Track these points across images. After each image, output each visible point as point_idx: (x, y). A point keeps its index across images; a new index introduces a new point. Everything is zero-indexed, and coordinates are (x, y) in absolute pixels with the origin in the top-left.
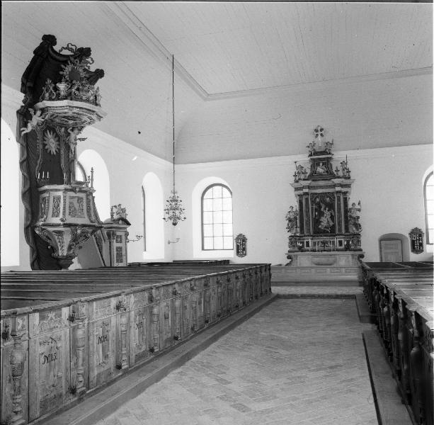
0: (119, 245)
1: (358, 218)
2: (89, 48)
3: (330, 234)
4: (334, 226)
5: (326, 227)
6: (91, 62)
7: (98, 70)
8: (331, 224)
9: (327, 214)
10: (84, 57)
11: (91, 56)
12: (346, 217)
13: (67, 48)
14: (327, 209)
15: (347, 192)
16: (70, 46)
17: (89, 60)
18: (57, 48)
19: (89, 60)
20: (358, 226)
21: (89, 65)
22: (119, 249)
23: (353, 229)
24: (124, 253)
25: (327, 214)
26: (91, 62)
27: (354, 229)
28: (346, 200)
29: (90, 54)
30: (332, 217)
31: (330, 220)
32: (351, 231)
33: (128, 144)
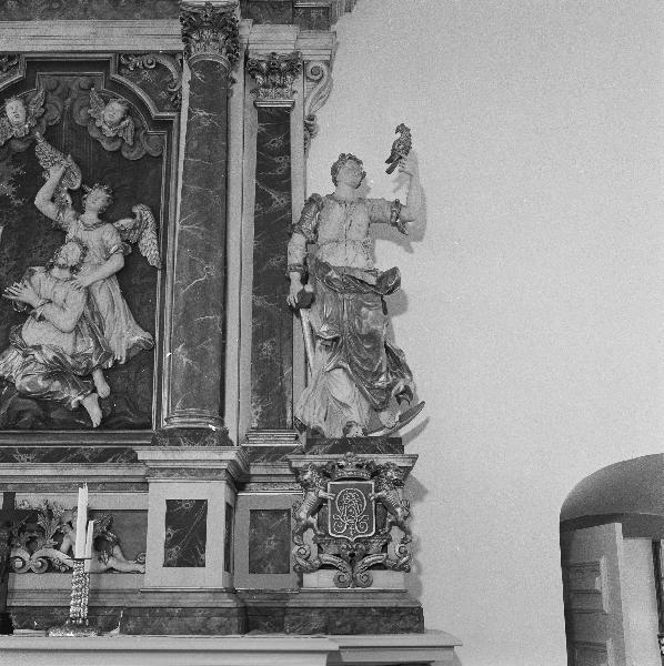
1: (387, 284)
3: (98, 444)
4: (143, 357)
5: (58, 370)
8: (124, 335)
9: (93, 243)
12: (270, 279)
14: (97, 198)
15: (294, 65)
20: (380, 368)
23: (328, 395)
25: (93, 243)
27: (343, 387)
28: (275, 125)
30: (135, 280)
31: (109, 299)
32: (306, 407)
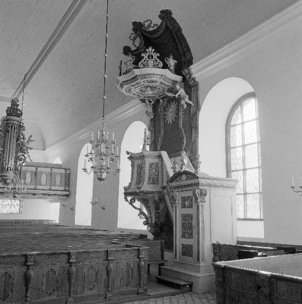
0: (186, 211)
2: (135, 24)
6: (149, 22)
7: (160, 16)
10: (143, 28)
11: (142, 22)
13: (134, 40)
16: (132, 38)
17: (146, 24)
18: (133, 48)
19: (146, 24)
21: (152, 25)
22: (187, 219)
24: (194, 223)
26: (149, 22)
29: (140, 23)
33: (275, 18)
